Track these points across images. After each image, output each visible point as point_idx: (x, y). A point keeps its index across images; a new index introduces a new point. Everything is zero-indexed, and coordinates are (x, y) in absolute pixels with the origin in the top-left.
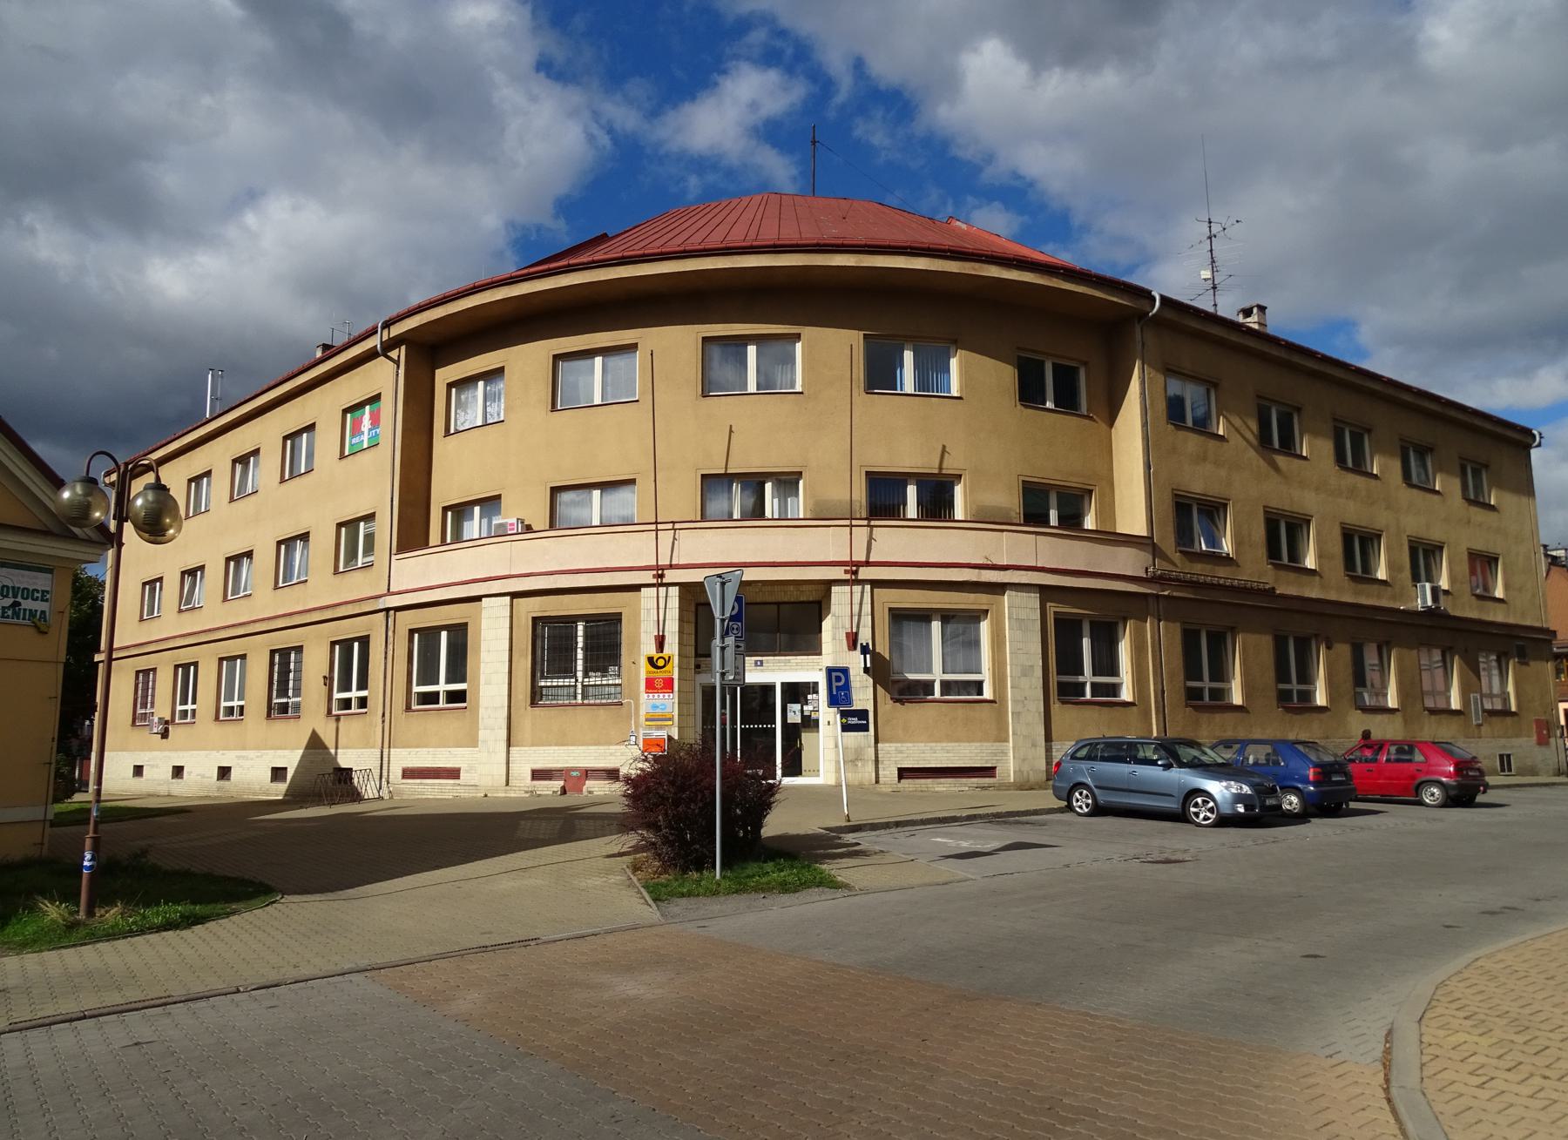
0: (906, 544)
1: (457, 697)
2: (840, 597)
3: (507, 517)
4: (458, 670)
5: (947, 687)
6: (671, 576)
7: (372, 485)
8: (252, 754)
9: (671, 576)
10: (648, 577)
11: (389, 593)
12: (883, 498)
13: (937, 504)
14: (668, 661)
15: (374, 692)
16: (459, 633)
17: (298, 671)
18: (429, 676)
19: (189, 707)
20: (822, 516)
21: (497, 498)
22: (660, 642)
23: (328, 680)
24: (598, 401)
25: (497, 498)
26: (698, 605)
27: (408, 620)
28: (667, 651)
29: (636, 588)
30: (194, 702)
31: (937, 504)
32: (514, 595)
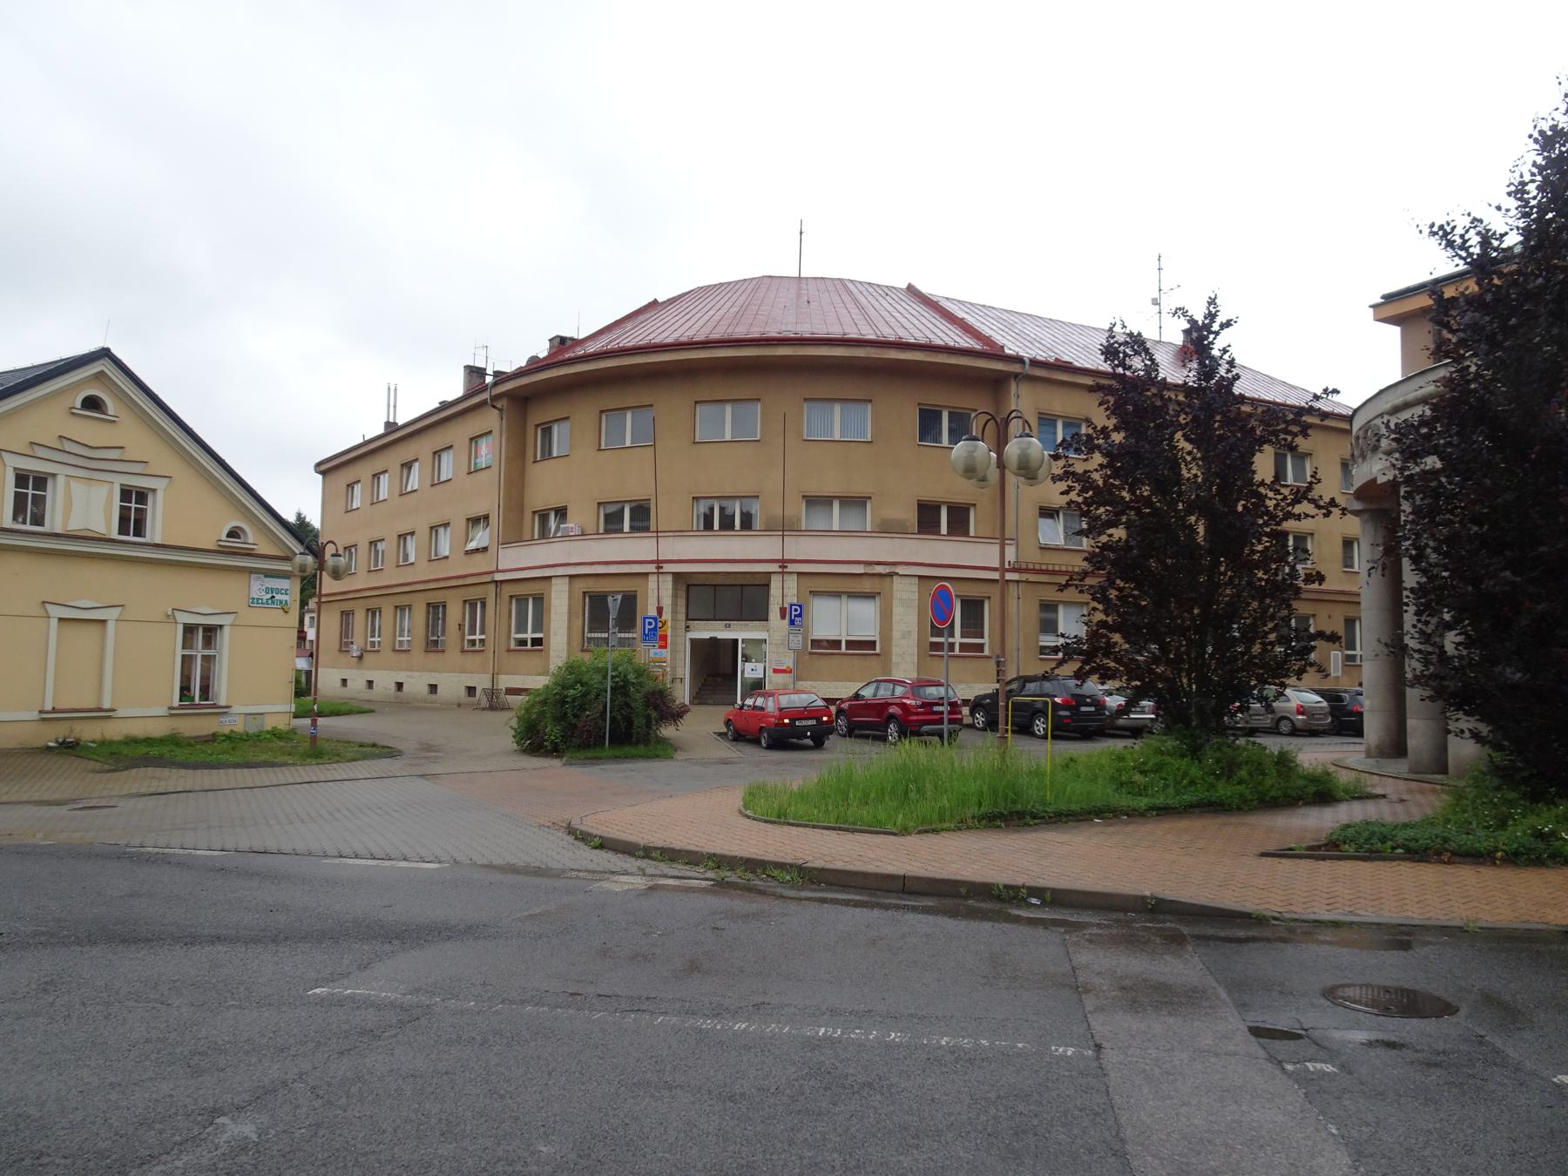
0: (943, 551)
1: (537, 642)
2: (775, 584)
3: (571, 525)
4: (539, 625)
5: (963, 647)
6: (668, 568)
7: (487, 499)
8: (417, 674)
9: (668, 568)
10: (651, 568)
11: (498, 571)
12: (927, 519)
13: (959, 524)
14: (664, 624)
15: (489, 636)
16: (539, 600)
17: (444, 620)
18: (522, 627)
19: (376, 639)
20: (887, 529)
21: (565, 508)
22: (660, 610)
23: (461, 626)
24: (728, 437)
25: (565, 508)
26: (688, 586)
27: (508, 590)
28: (664, 617)
29: (646, 574)
30: (482, 632)
31: (959, 524)
32: (571, 577)
